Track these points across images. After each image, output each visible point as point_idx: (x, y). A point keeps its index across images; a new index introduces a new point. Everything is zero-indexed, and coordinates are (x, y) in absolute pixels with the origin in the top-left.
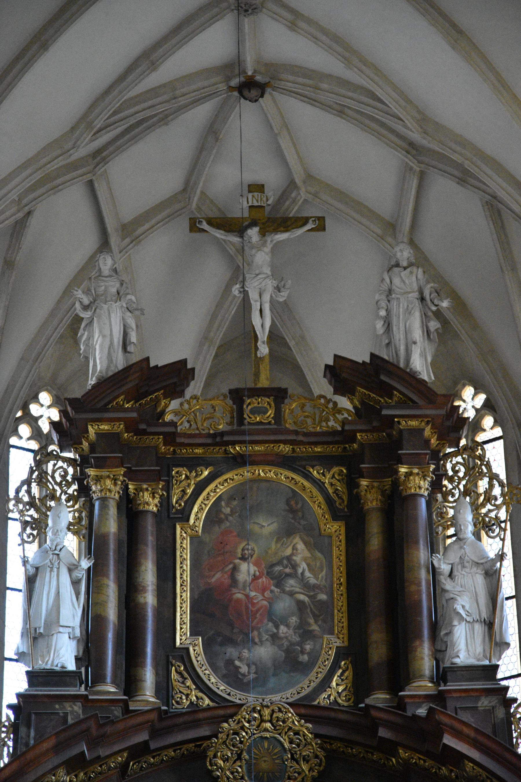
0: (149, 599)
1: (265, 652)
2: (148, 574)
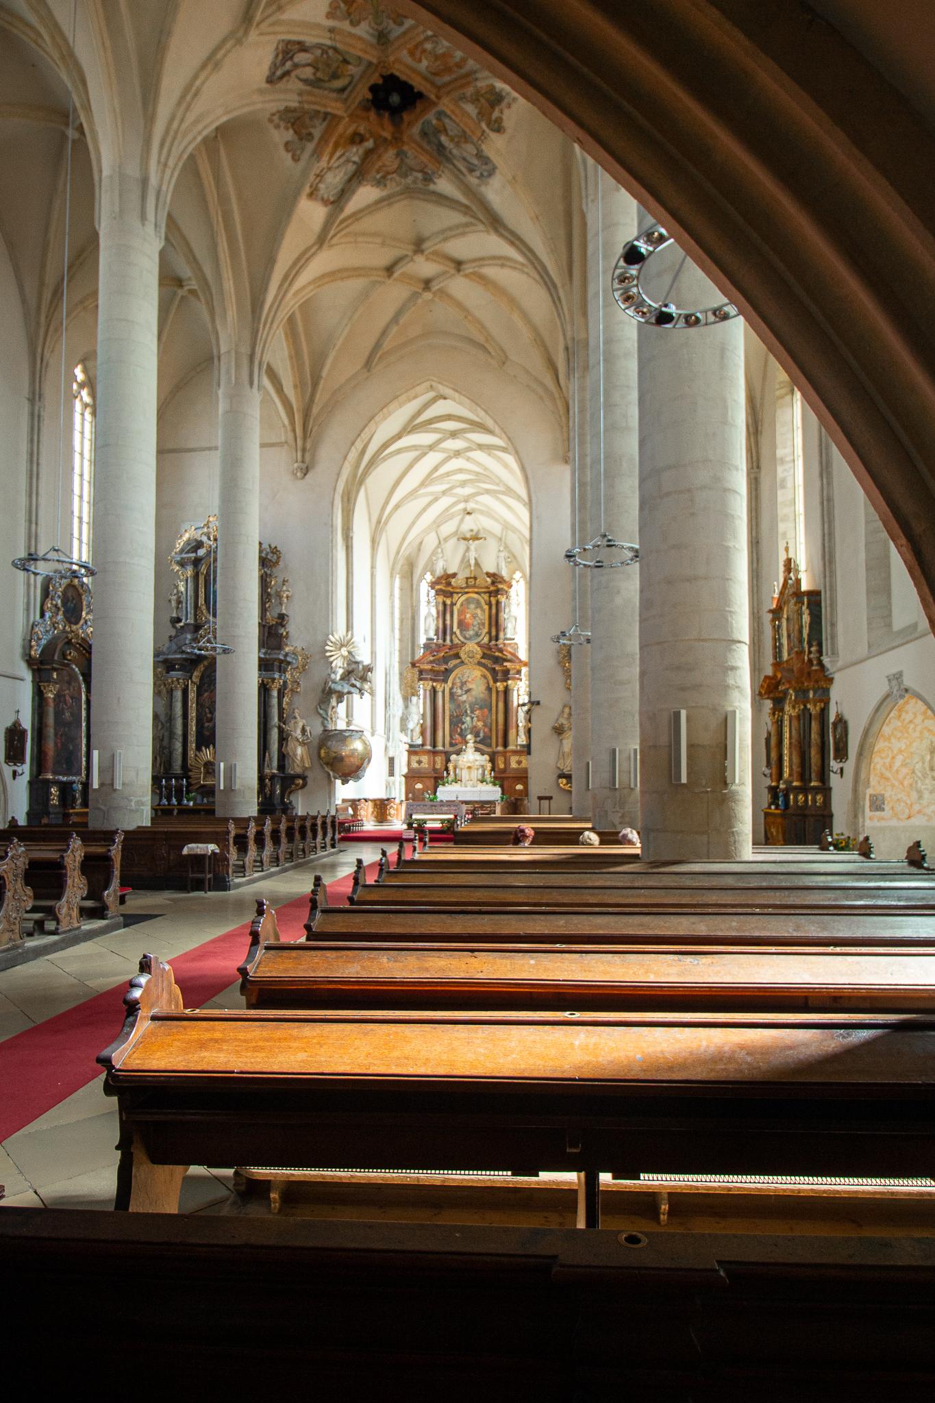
0: (448, 622)
1: (471, 633)
2: (448, 617)
